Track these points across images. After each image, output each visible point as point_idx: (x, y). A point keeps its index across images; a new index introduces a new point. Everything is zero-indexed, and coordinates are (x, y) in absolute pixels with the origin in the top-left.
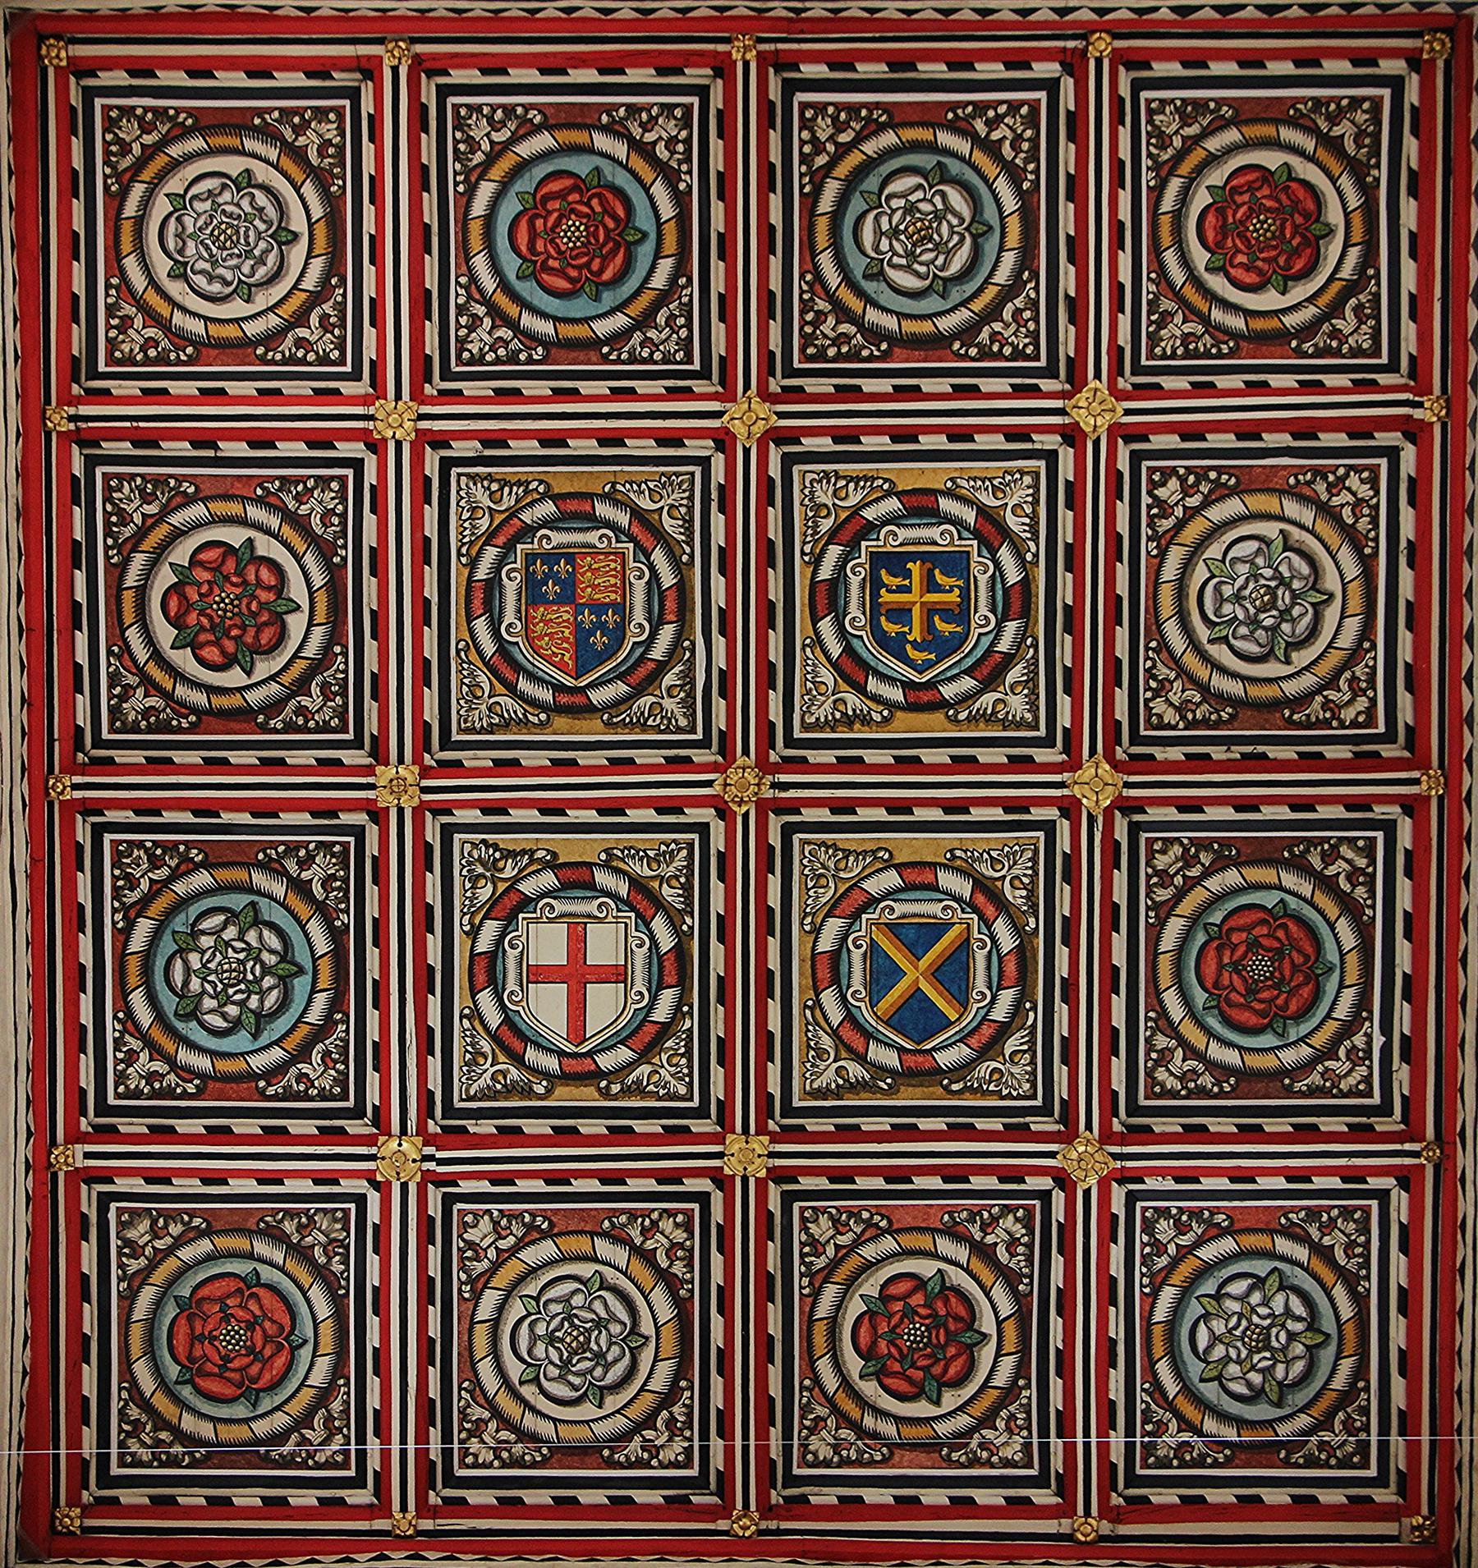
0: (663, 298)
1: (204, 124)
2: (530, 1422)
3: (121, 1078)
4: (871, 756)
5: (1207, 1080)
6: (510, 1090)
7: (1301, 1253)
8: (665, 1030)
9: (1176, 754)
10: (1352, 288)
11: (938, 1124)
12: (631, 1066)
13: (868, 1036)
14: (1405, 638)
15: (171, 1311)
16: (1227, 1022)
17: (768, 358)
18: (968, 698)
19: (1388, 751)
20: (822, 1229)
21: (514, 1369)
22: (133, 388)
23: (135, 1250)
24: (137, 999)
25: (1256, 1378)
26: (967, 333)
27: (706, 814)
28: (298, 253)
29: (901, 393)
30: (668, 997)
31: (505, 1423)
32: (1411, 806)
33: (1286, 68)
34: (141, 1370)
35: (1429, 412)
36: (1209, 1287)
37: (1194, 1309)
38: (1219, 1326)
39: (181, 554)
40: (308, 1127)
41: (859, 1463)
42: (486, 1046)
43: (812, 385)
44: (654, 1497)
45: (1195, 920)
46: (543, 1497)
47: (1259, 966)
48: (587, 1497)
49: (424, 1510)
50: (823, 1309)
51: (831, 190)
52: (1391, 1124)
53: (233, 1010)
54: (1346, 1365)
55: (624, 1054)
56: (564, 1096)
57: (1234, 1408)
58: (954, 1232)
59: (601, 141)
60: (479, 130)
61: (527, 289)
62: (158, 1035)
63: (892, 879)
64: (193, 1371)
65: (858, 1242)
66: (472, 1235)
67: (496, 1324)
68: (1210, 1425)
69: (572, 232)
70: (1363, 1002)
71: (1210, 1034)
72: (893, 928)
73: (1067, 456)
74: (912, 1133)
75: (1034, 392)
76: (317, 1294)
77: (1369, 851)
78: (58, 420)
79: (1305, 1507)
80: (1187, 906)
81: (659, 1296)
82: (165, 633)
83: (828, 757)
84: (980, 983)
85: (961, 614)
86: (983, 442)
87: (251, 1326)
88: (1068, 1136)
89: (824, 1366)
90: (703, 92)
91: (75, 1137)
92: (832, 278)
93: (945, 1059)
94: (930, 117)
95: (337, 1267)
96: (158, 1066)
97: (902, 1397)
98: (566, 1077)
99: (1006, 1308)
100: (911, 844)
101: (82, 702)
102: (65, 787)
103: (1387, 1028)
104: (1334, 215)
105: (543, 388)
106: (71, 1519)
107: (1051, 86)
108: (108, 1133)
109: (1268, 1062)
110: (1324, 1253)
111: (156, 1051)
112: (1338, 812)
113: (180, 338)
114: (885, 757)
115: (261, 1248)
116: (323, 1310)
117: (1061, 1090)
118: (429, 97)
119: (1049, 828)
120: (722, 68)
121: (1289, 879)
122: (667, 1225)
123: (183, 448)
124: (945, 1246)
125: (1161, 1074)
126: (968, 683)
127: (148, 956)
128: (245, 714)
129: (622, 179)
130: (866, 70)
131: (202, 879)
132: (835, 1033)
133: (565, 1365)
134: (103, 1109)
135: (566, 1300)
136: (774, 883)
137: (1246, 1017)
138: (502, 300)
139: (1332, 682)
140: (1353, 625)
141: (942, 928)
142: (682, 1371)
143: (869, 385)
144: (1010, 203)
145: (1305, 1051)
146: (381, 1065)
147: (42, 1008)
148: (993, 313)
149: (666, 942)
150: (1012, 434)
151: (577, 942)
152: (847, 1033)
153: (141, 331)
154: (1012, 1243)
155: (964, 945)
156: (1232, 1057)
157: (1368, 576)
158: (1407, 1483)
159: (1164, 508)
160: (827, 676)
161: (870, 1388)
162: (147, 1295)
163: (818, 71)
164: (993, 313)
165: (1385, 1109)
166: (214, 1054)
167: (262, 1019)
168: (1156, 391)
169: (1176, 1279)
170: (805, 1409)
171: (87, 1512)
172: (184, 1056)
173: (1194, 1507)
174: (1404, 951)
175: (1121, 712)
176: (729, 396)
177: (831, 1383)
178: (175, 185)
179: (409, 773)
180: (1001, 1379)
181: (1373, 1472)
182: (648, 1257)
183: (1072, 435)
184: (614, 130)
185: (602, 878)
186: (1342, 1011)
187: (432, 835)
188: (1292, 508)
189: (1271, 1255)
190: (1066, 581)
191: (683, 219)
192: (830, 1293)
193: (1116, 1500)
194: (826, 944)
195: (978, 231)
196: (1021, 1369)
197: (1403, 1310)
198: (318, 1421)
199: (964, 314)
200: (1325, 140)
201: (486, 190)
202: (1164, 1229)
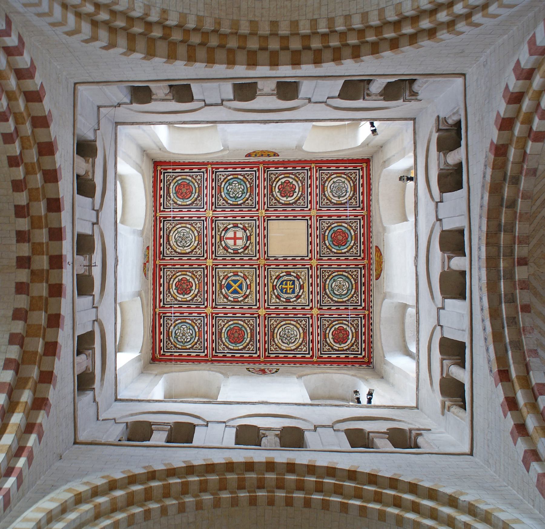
0: (331, 250)
1: (355, 186)
3: (220, 175)
4: (266, 280)
5: (220, 327)
6: (219, 229)
7: (196, 341)
8: (227, 251)
9: (266, 323)
10: (332, 348)
11: (214, 289)
12: (222, 246)
13: (226, 280)
14: (283, 355)
16: (228, 331)
17: (322, 265)
18: (274, 294)
19: (267, 353)
20: (199, 273)
21: (180, 230)
22: (318, 176)
24: (231, 177)
25: (178, 334)
26: (326, 294)
27: (258, 257)
28: (337, 199)
29: (318, 284)
30: (232, 251)
32: (259, 356)
33: (363, 339)
34: (180, 178)
35: (315, 359)
36: (191, 328)
37: (188, 326)
38: (185, 329)
39: (294, 183)
40: (214, 201)
41: (166, 278)
42: (225, 226)
43: (319, 271)
44: (162, 249)
45: (243, 326)
46: (162, 234)
47: (236, 335)
48: (162, 240)
49: (160, 217)
50: (188, 273)
51: (346, 274)
52: (214, 353)
54: (180, 347)
55: (224, 245)
56: (218, 237)
58: (199, 292)
59: (353, 242)
60: (354, 224)
61: (332, 231)
63: (249, 283)
64: (179, 185)
65: (197, 278)
67: (186, 227)
69: (340, 238)
70: (231, 349)
72: (242, 283)
73: (309, 308)
74: (213, 286)
75: (318, 303)
76: (190, 202)
77: (253, 350)
78: (313, 165)
79: (160, 341)
80: (245, 325)
81: (190, 250)
82: (283, 180)
83: (266, 274)
85: (286, 293)
86: (311, 296)
88: (212, 308)
89: (180, 273)
90: (360, 256)
91: (212, 168)
92: (334, 274)
93: (223, 290)
94: (356, 288)
95: (194, 205)
98: (221, 237)
99: (188, 299)
100: (253, 285)
101: (273, 169)
102: (261, 166)
103: (227, 353)
104: (343, 345)
105: (318, 233)
106: (159, 168)
107: (361, 305)
108: (213, 173)
109: (223, 336)
110: (196, 344)
112: (258, 346)
113: (325, 182)
114: (266, 282)
115: (197, 194)
116: (188, 203)
117: (219, 307)
118: (359, 217)
119: (256, 305)
120: (363, 259)
121: (249, 339)
122: (200, 251)
123: (309, 183)
124: (197, 290)
125: (221, 321)
126: (276, 294)
127: (237, 178)
128: (272, 191)
129: (348, 245)
130: (363, 279)
131: (248, 186)
132: (227, 275)
133: (180, 237)
134: (216, 172)
135: (189, 237)
136: (248, 266)
138: (330, 228)
139: (276, 345)
140: (285, 348)
141: (242, 290)
142: (179, 253)
143: (319, 280)
144: (344, 300)
145: (224, 341)
146: (222, 211)
147: (230, 163)
148: (329, 297)
150: (312, 300)
151: (240, 238)
152: (227, 277)
153: (326, 177)
156: (223, 331)
157: (292, 350)
158: (164, 355)
159: (301, 321)
160: (277, 274)
161: (177, 280)
162: (190, 178)
163: (363, 272)
164: (329, 297)
167: (229, 194)
168: (318, 320)
171: (160, 170)
172: (223, 183)
173: (160, 325)
174: (239, 355)
175: (272, 315)
176: (317, 260)
177: (178, 274)
178: (346, 182)
179: (264, 215)
180: (178, 298)
182: (195, 248)
183: (312, 308)
184: (354, 243)
185: (249, 242)
186: (230, 347)
187: (255, 218)
188: (301, 339)
190: (291, 307)
191: (342, 253)
192: (190, 274)
193: (161, 314)
194: (239, 274)
195: (340, 295)
196: (179, 301)
199: (329, 293)
200: (353, 344)
201: (346, 225)
202: (199, 321)
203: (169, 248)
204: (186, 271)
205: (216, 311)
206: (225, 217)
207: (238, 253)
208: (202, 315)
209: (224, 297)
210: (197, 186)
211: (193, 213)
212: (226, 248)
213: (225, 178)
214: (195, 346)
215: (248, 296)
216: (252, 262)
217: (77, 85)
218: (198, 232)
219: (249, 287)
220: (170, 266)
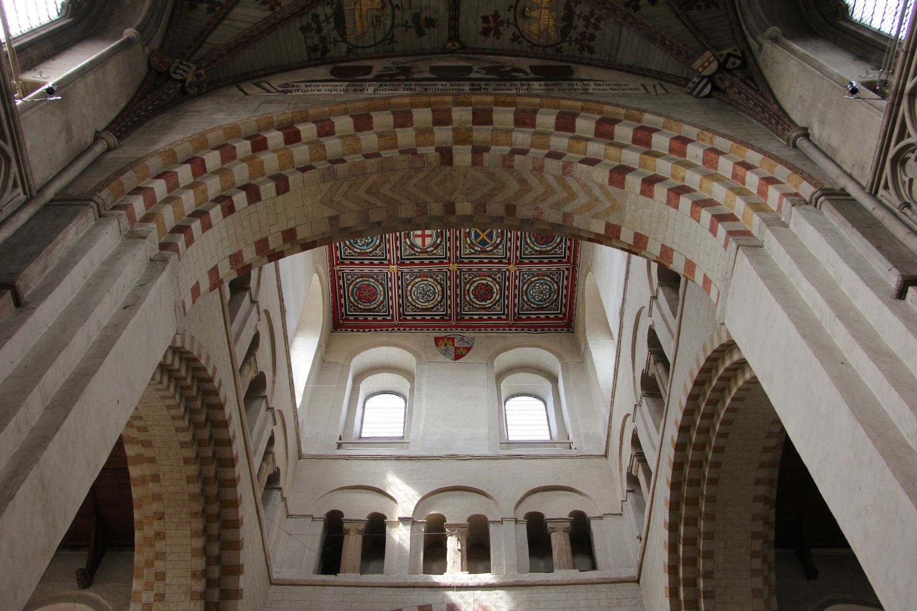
2: (417, 305)
3: (344, 253)
5: (534, 253)
7: (549, 279)
12: (433, 250)
13: (475, 245)
15: (355, 289)
16: (538, 243)
20: (467, 276)
21: (414, 298)
23: (349, 280)
25: (540, 298)
31: (413, 305)
34: (351, 298)
36: (533, 285)
37: (530, 288)
38: (534, 291)
41: (473, 311)
42: (408, 248)
50: (467, 288)
53: (363, 242)
54: (556, 296)
55: (432, 249)
57: (536, 303)
58: (490, 276)
62: (350, 246)
64: (360, 298)
65: (473, 278)
66: (406, 277)
67: (411, 291)
68: (532, 305)
71: (535, 245)
76: (380, 287)
79: (547, 318)
81: (439, 286)
84: (495, 237)
87: (369, 295)
89: (467, 297)
91: (338, 264)
93: (488, 249)
95: (383, 282)
96: (351, 251)
97: (480, 301)
98: (422, 252)
99: (498, 288)
103: (565, 244)
108: (343, 263)
109: (545, 249)
110: (553, 279)
111: (350, 249)
115: (370, 280)
116: (381, 289)
122: (440, 275)
124: (488, 278)
125: (526, 252)
132: (469, 245)
133: (423, 297)
134: (342, 259)
135: (423, 287)
137: (540, 242)
145: (551, 248)
152: (471, 245)
154: (499, 278)
156: (538, 249)
158: (564, 314)
162: (351, 287)
166: (360, 249)
167: (368, 244)
169: (528, 283)
170: (464, 303)
171: (344, 320)
172: (355, 250)
173: (529, 319)
177: (468, 299)
181: (559, 312)
186: (558, 241)
189: (544, 279)
192: (468, 286)
193: (516, 318)
196: (500, 297)
197: (566, 279)
198: (381, 306)
203: (437, 309)
204: (464, 290)
205: (513, 259)
208: (518, 274)
209: (496, 247)
210: (361, 279)
211: (393, 284)
212: (436, 246)
213: (349, 248)
214: (556, 279)
217: (273, 581)
218: (417, 277)
220: (459, 309)
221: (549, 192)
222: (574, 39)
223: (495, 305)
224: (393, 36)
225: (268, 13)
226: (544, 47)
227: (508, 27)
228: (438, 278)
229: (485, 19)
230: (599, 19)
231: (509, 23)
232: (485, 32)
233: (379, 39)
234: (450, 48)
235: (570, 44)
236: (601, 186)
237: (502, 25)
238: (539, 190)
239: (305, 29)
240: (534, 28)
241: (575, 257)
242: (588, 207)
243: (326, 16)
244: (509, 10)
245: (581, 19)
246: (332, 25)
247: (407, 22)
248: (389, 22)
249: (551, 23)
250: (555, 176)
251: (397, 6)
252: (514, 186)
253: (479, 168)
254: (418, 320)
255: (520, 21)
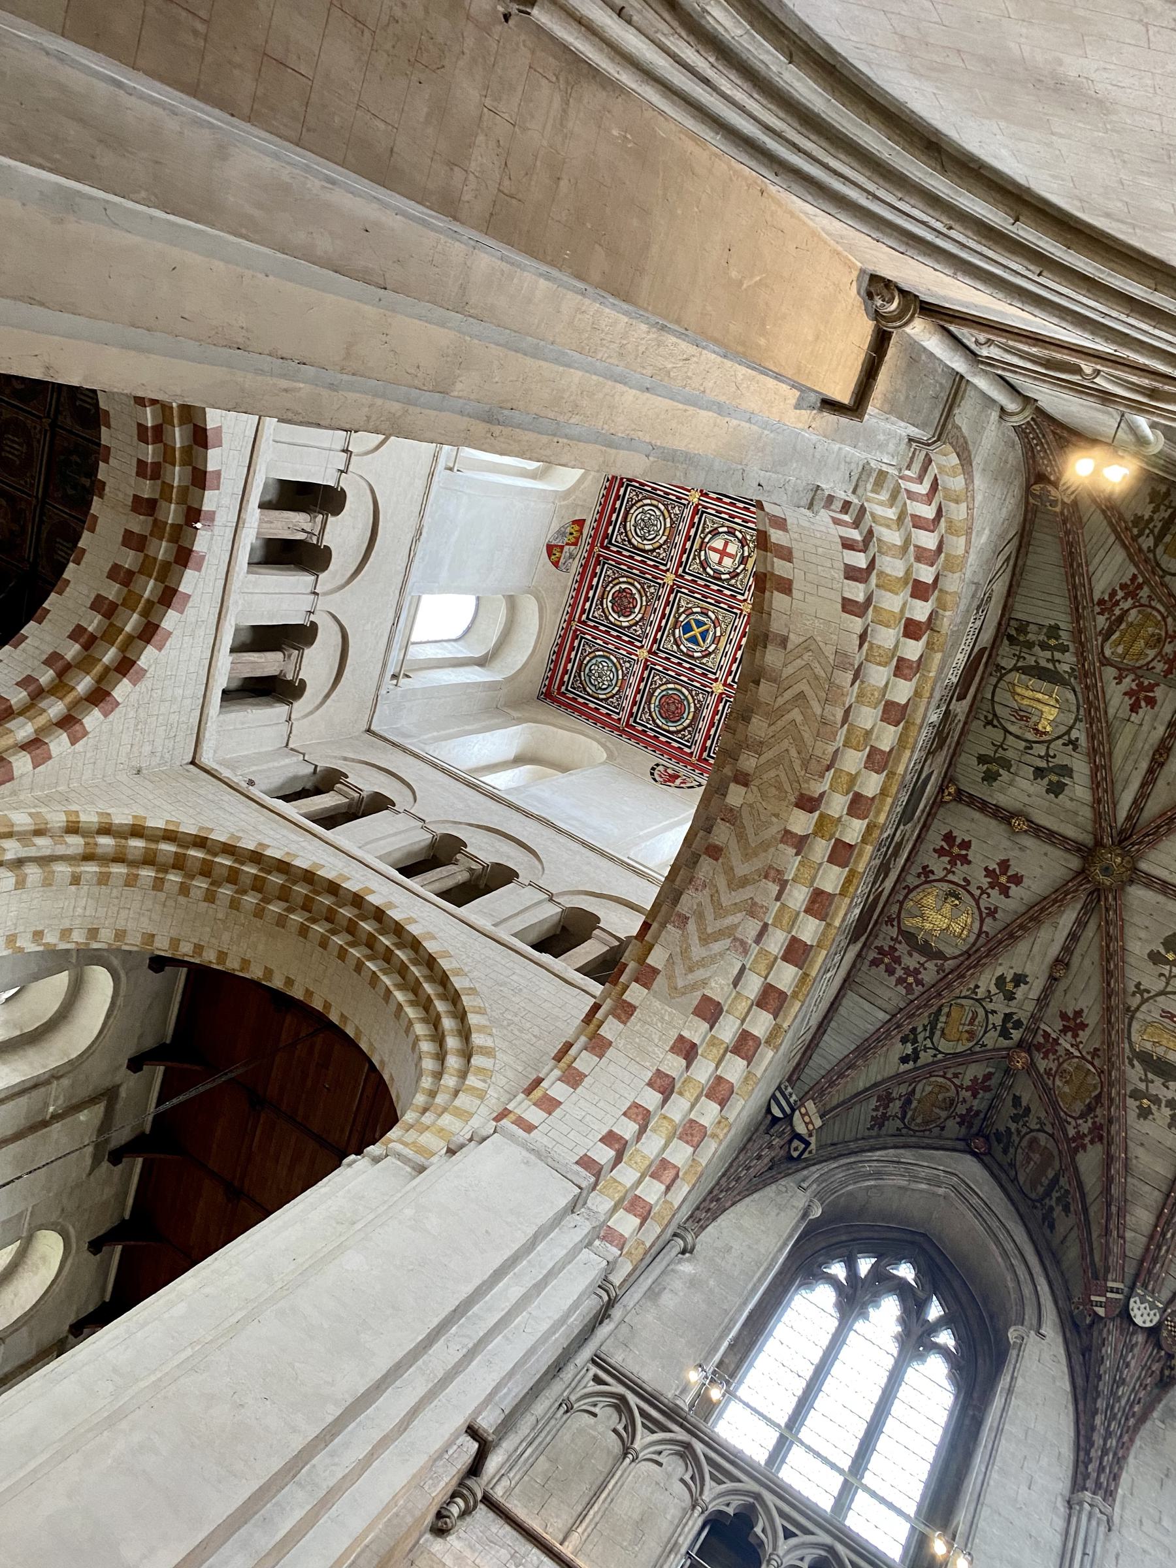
6: (704, 529)
8: (704, 569)
11: (663, 624)
13: (688, 616)
20: (652, 590)
21: (646, 508)
30: (711, 573)
31: (637, 502)
44: (610, 531)
47: (673, 708)
55: (703, 558)
58: (642, 618)
63: (718, 634)
67: (657, 507)
70: (658, 727)
72: (707, 630)
79: (565, 672)
80: (690, 697)
81: (650, 547)
88: (650, 652)
89: (624, 579)
110: (612, 697)
121: (688, 722)
124: (640, 616)
141: (704, 641)
149: (724, 577)
151: (730, 555)
155: (698, 645)
158: (563, 694)
161: (617, 588)
165: (635, 721)
173: (572, 648)
177: (622, 580)
182: (659, 548)
185: (742, 567)
192: (639, 586)
194: (710, 614)
196: (611, 623)
202: (628, 665)
205: (653, 658)
206: (717, 511)
207: (720, 579)
212: (704, 565)
215: (710, 654)
216: (733, 602)
218: (672, 522)
219: (716, 640)
221: (720, 911)
222: (897, 946)
223: (603, 611)
224: (995, 726)
225: (1097, 596)
226: (901, 903)
227: (945, 869)
228: (661, 551)
229: (966, 845)
230: (909, 989)
231: (949, 872)
232: (949, 838)
233: (998, 709)
234: (947, 788)
235: (892, 939)
236: (704, 983)
237: (949, 862)
238: (727, 899)
239: (1053, 631)
240: (930, 900)
241: (631, 736)
242: (685, 952)
243: (1059, 662)
244: (965, 879)
245: (918, 966)
246: (1043, 663)
247: (1005, 750)
248: (1012, 729)
249: (928, 926)
250: (736, 926)
251: (1031, 748)
252: (742, 869)
253: (779, 836)
254: (614, 503)
255: (946, 886)
